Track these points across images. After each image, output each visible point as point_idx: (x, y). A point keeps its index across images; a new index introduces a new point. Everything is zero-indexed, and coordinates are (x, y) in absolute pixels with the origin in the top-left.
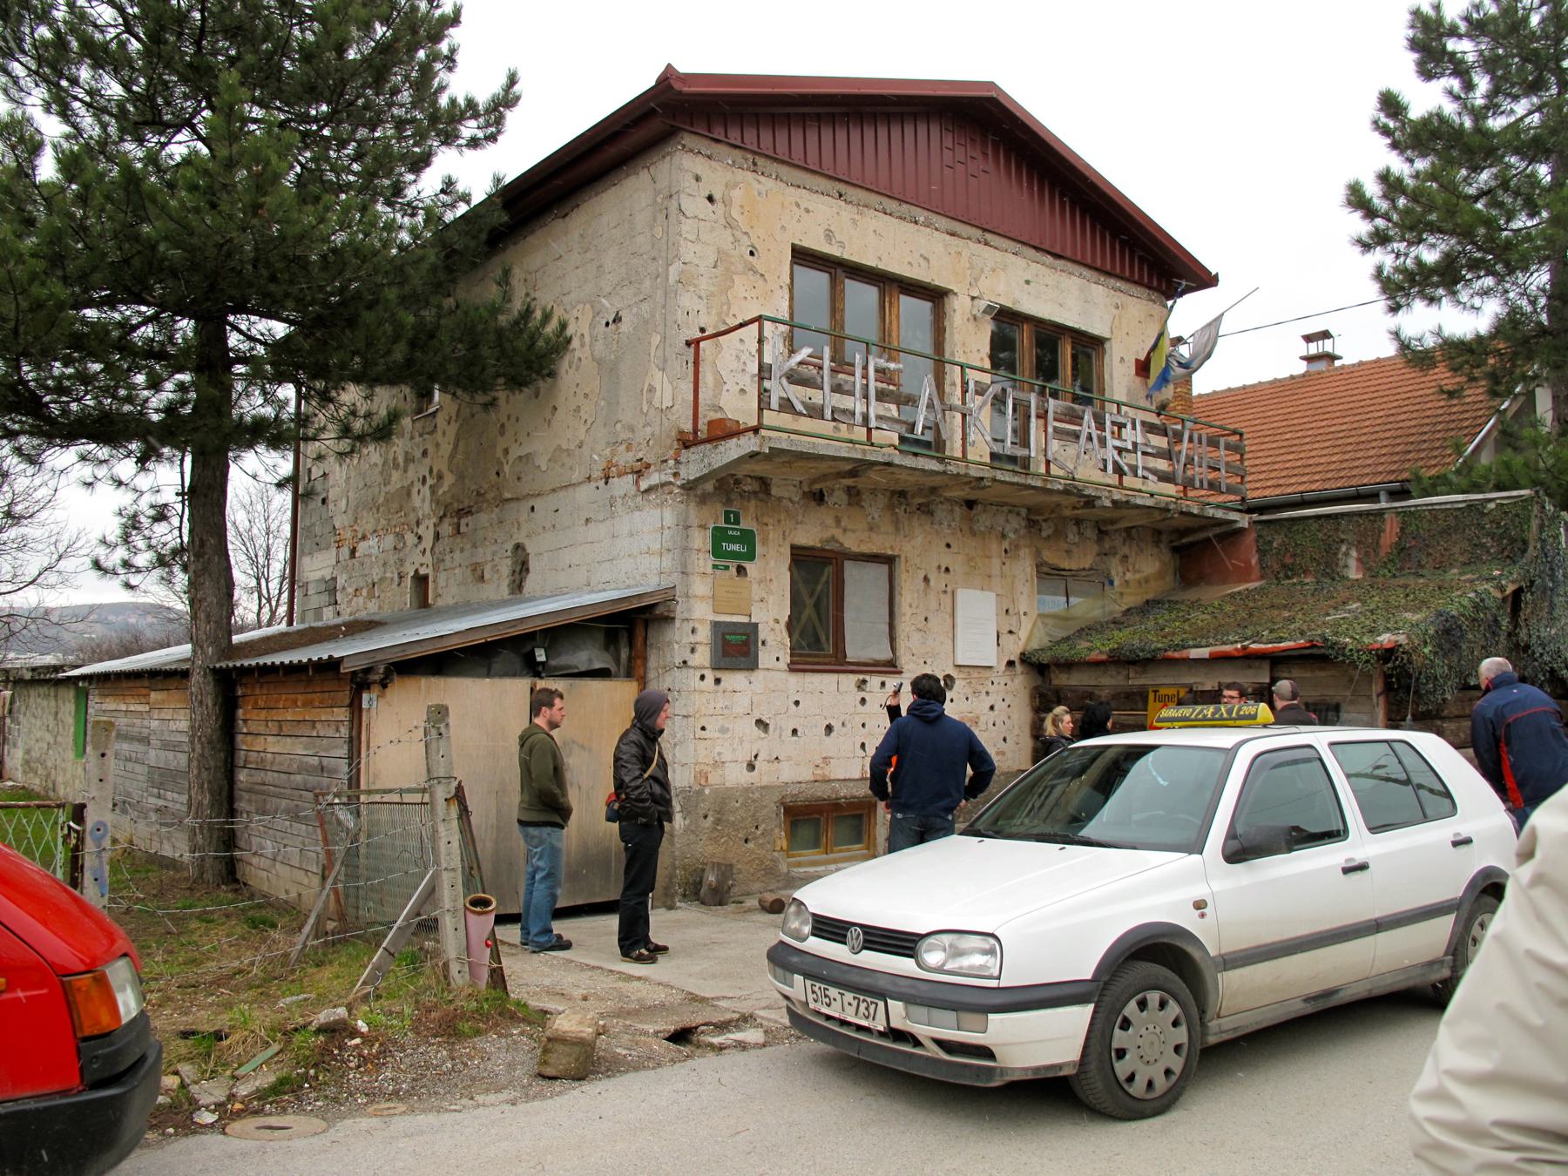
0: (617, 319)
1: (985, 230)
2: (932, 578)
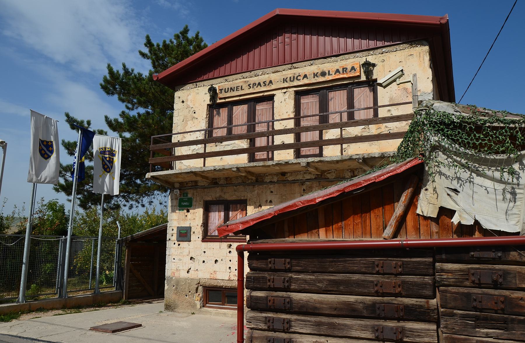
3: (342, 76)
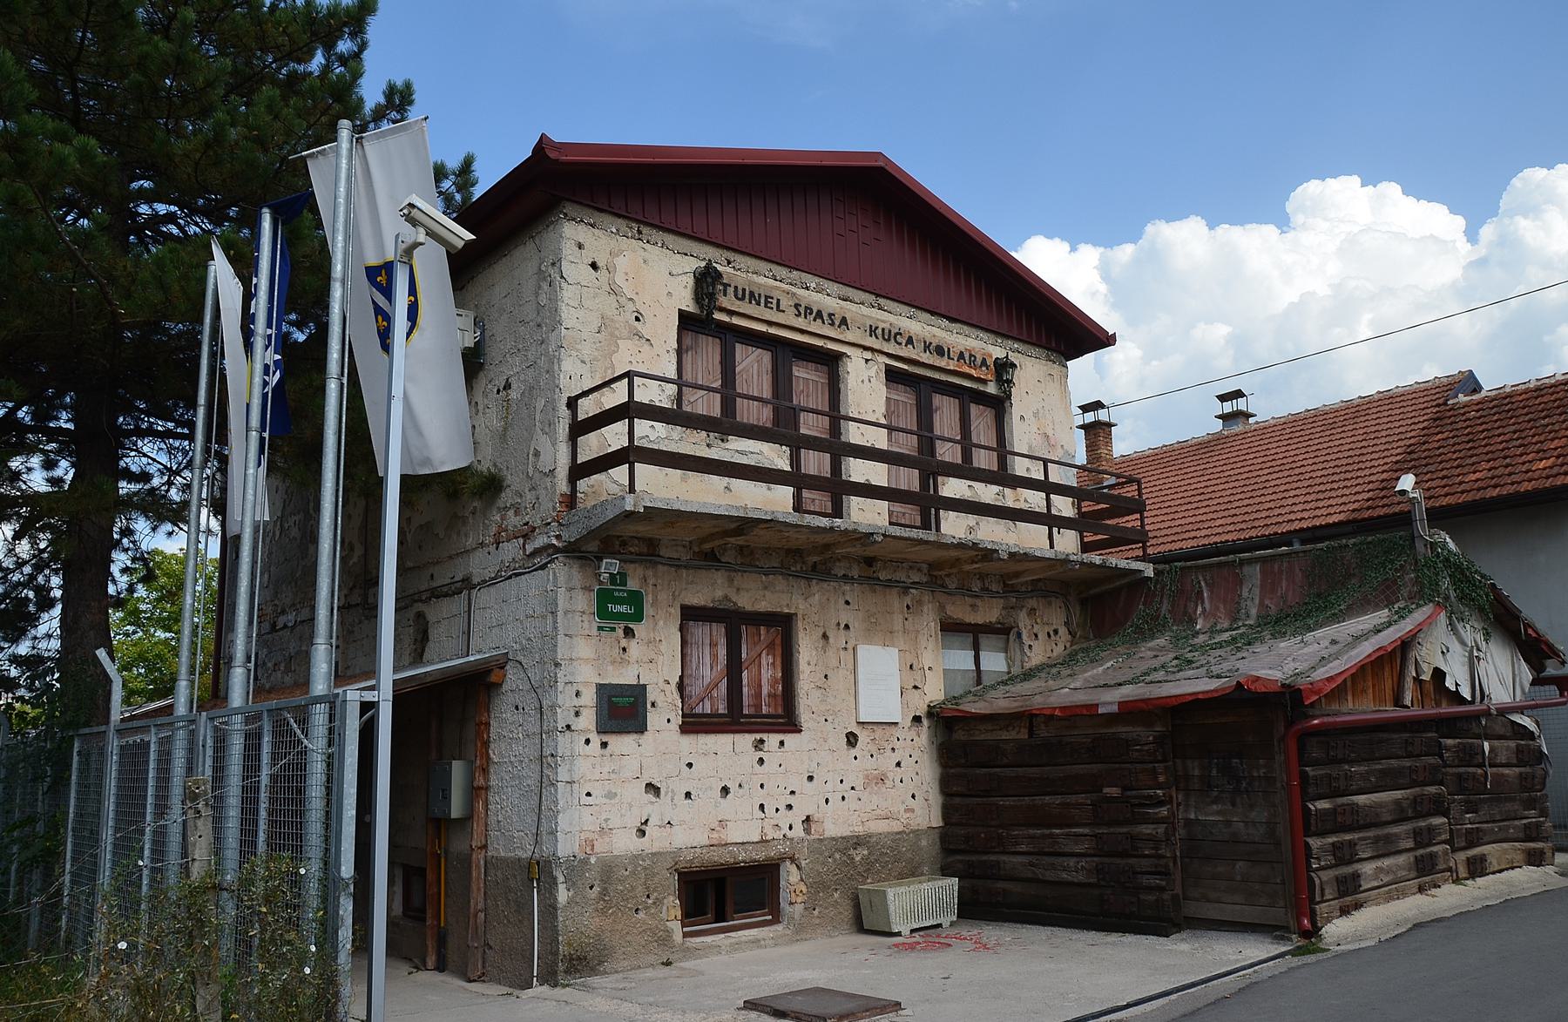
0: (507, 386)
1: (877, 295)
2: (831, 634)
3: (966, 369)
